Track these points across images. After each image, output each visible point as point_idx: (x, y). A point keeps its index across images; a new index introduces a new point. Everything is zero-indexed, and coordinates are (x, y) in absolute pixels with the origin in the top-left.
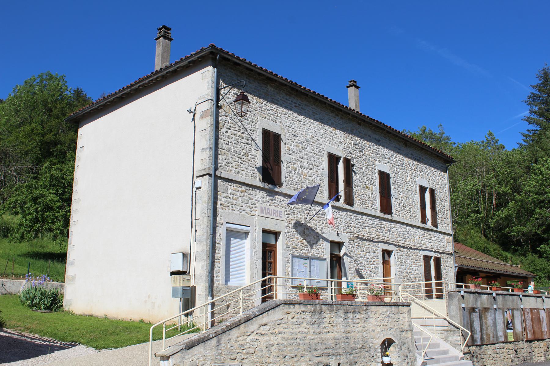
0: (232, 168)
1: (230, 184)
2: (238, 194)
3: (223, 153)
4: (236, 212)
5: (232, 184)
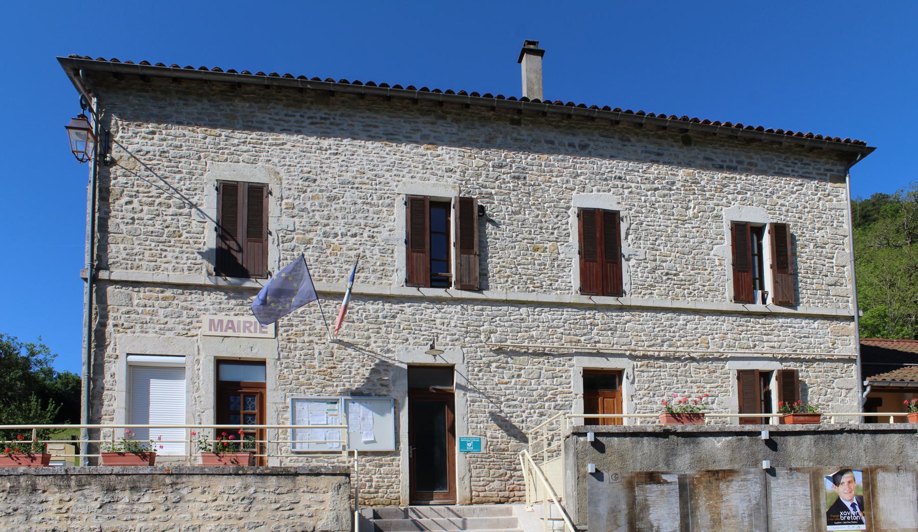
0: (142, 263)
1: (137, 289)
2: (156, 303)
3: (120, 240)
4: (151, 335)
5: (142, 289)
